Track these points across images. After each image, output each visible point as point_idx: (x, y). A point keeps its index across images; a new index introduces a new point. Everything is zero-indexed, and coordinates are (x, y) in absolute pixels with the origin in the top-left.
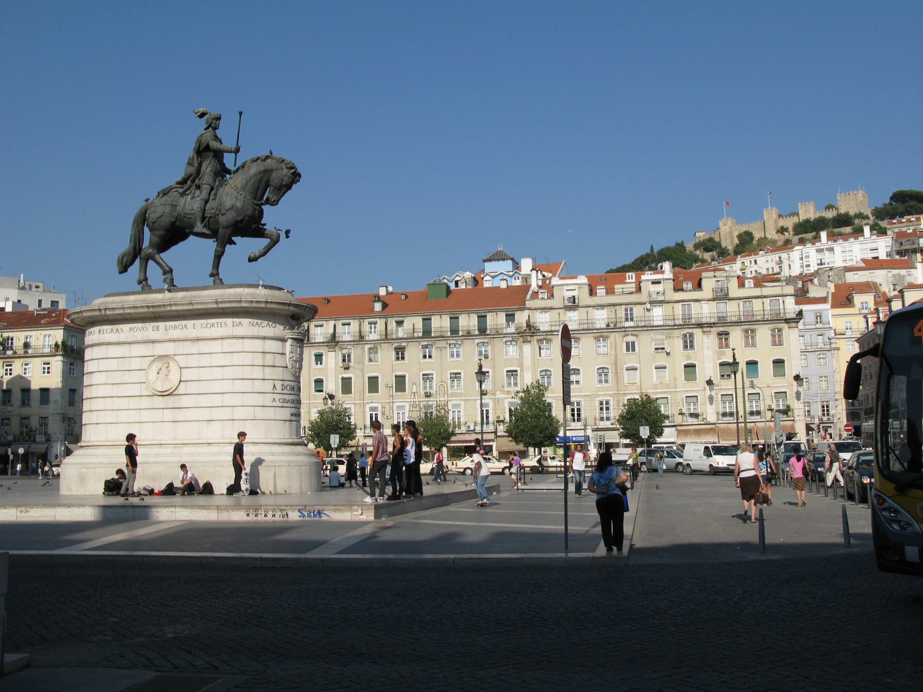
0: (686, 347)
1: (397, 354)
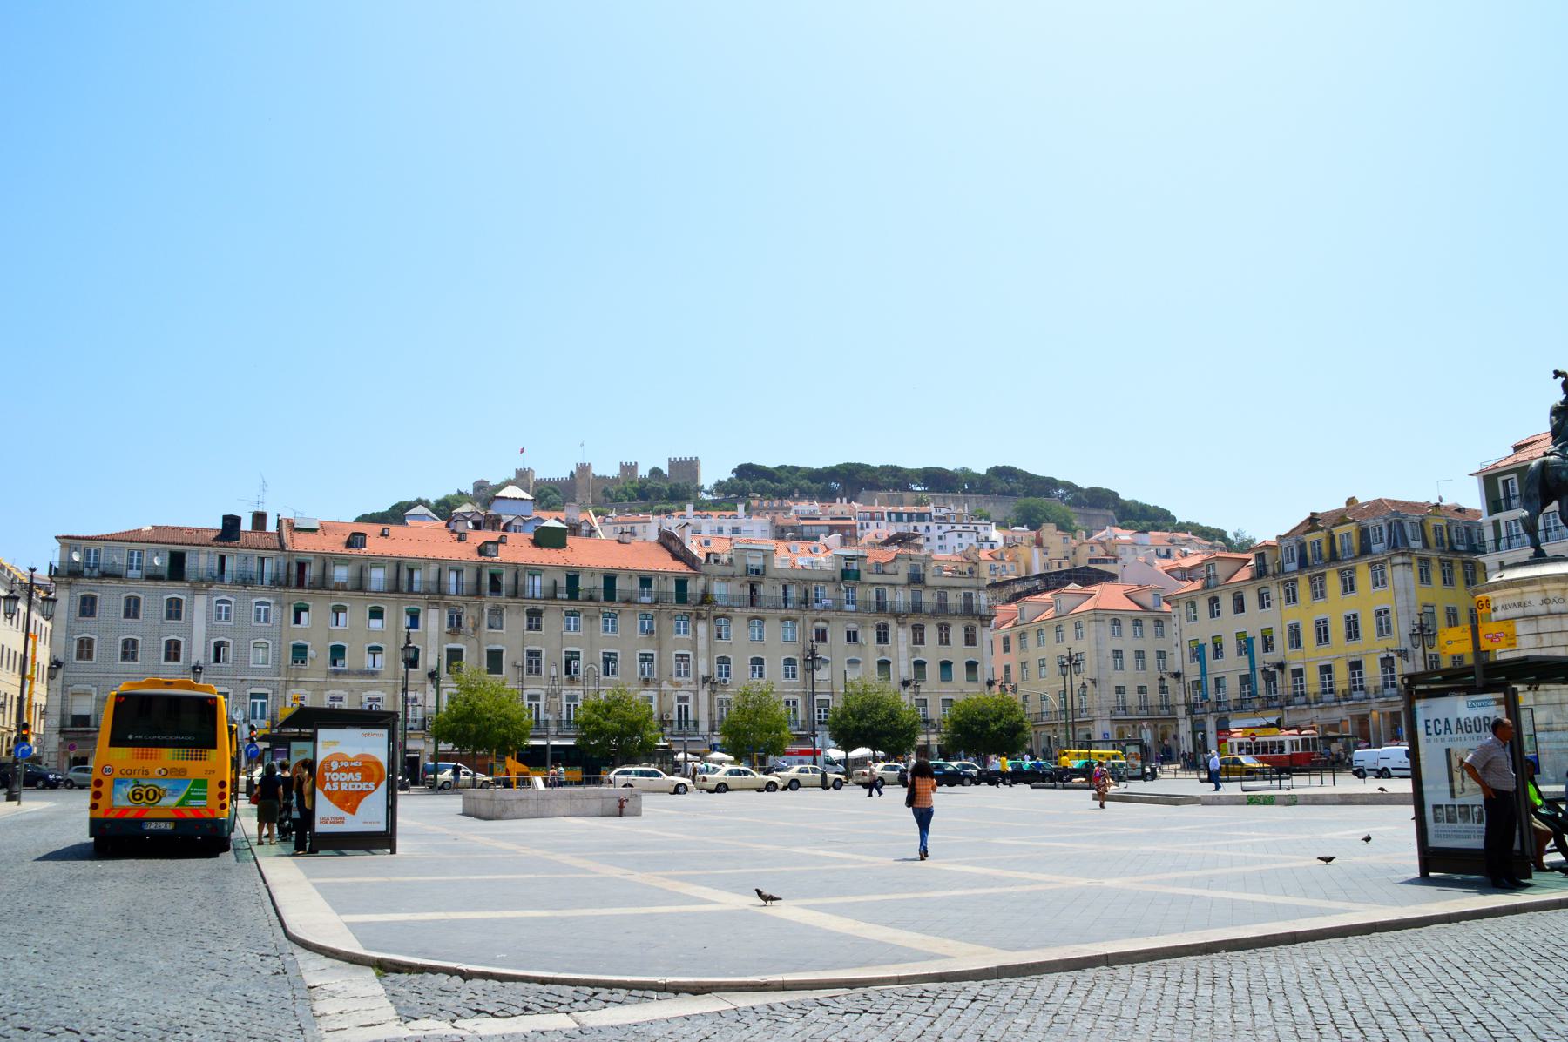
0: (879, 640)
1: (530, 620)
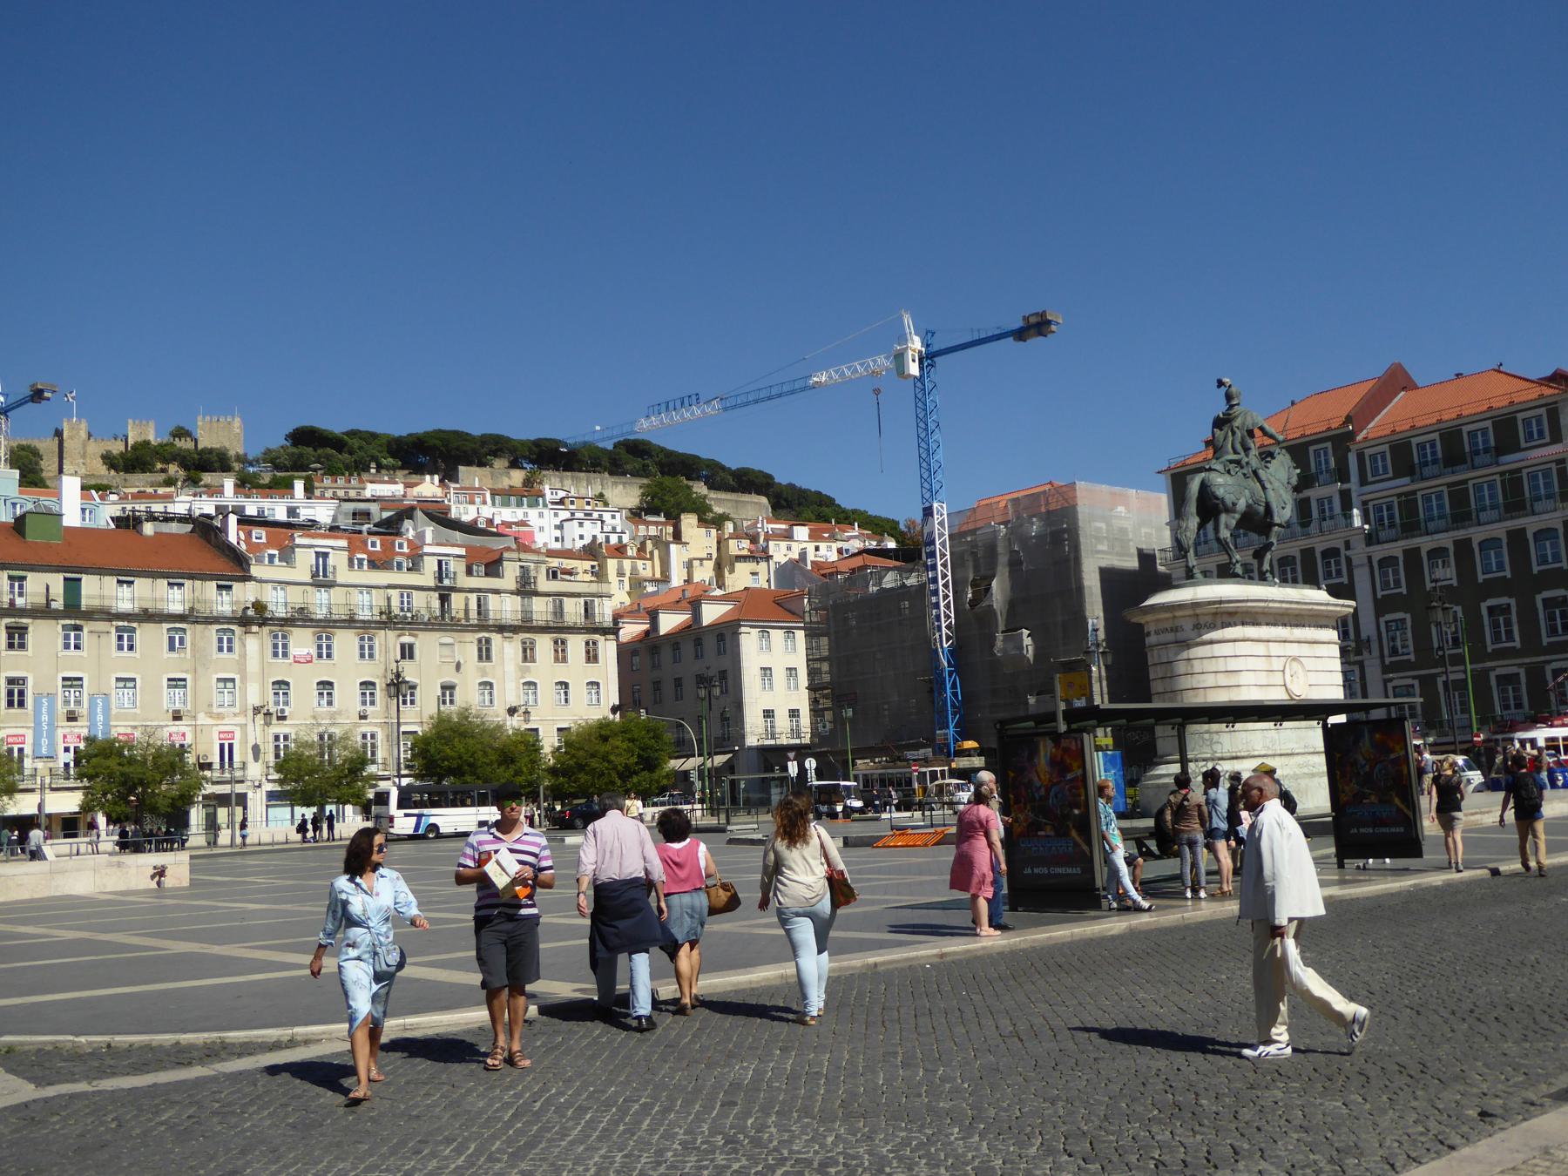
0: (480, 658)
1: (10, 637)
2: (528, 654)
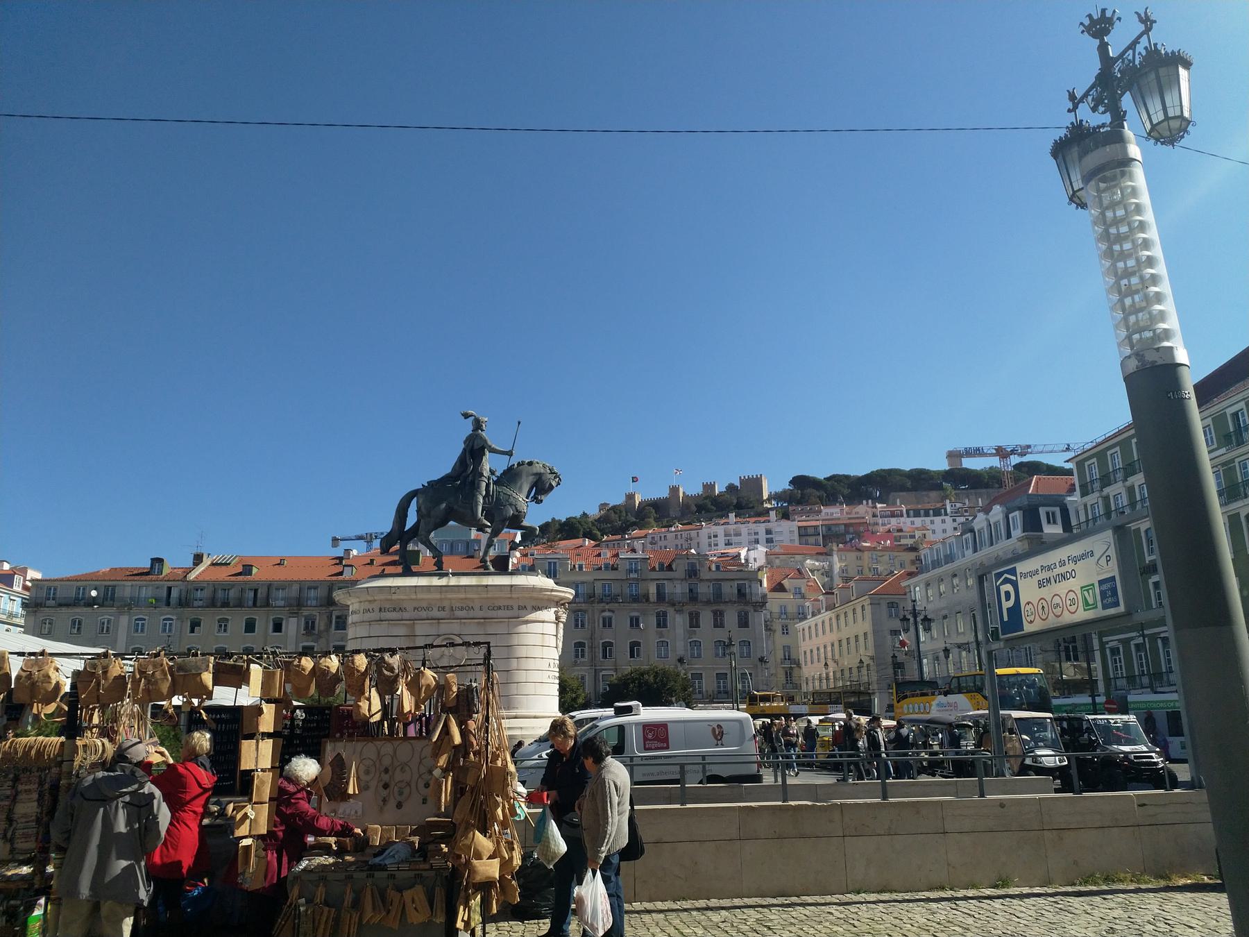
0: (659, 626)
2: (694, 621)
